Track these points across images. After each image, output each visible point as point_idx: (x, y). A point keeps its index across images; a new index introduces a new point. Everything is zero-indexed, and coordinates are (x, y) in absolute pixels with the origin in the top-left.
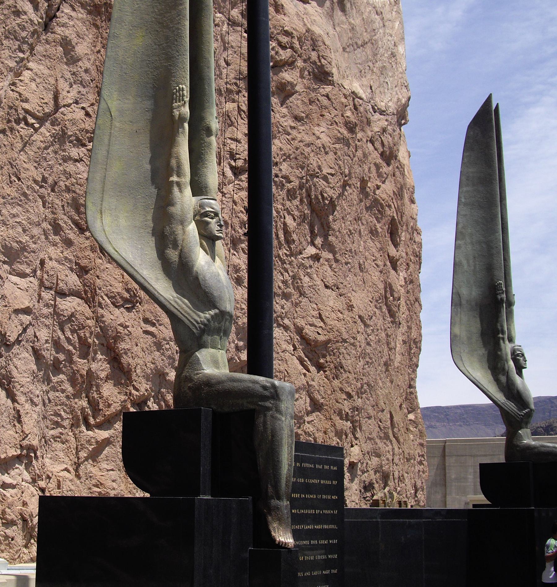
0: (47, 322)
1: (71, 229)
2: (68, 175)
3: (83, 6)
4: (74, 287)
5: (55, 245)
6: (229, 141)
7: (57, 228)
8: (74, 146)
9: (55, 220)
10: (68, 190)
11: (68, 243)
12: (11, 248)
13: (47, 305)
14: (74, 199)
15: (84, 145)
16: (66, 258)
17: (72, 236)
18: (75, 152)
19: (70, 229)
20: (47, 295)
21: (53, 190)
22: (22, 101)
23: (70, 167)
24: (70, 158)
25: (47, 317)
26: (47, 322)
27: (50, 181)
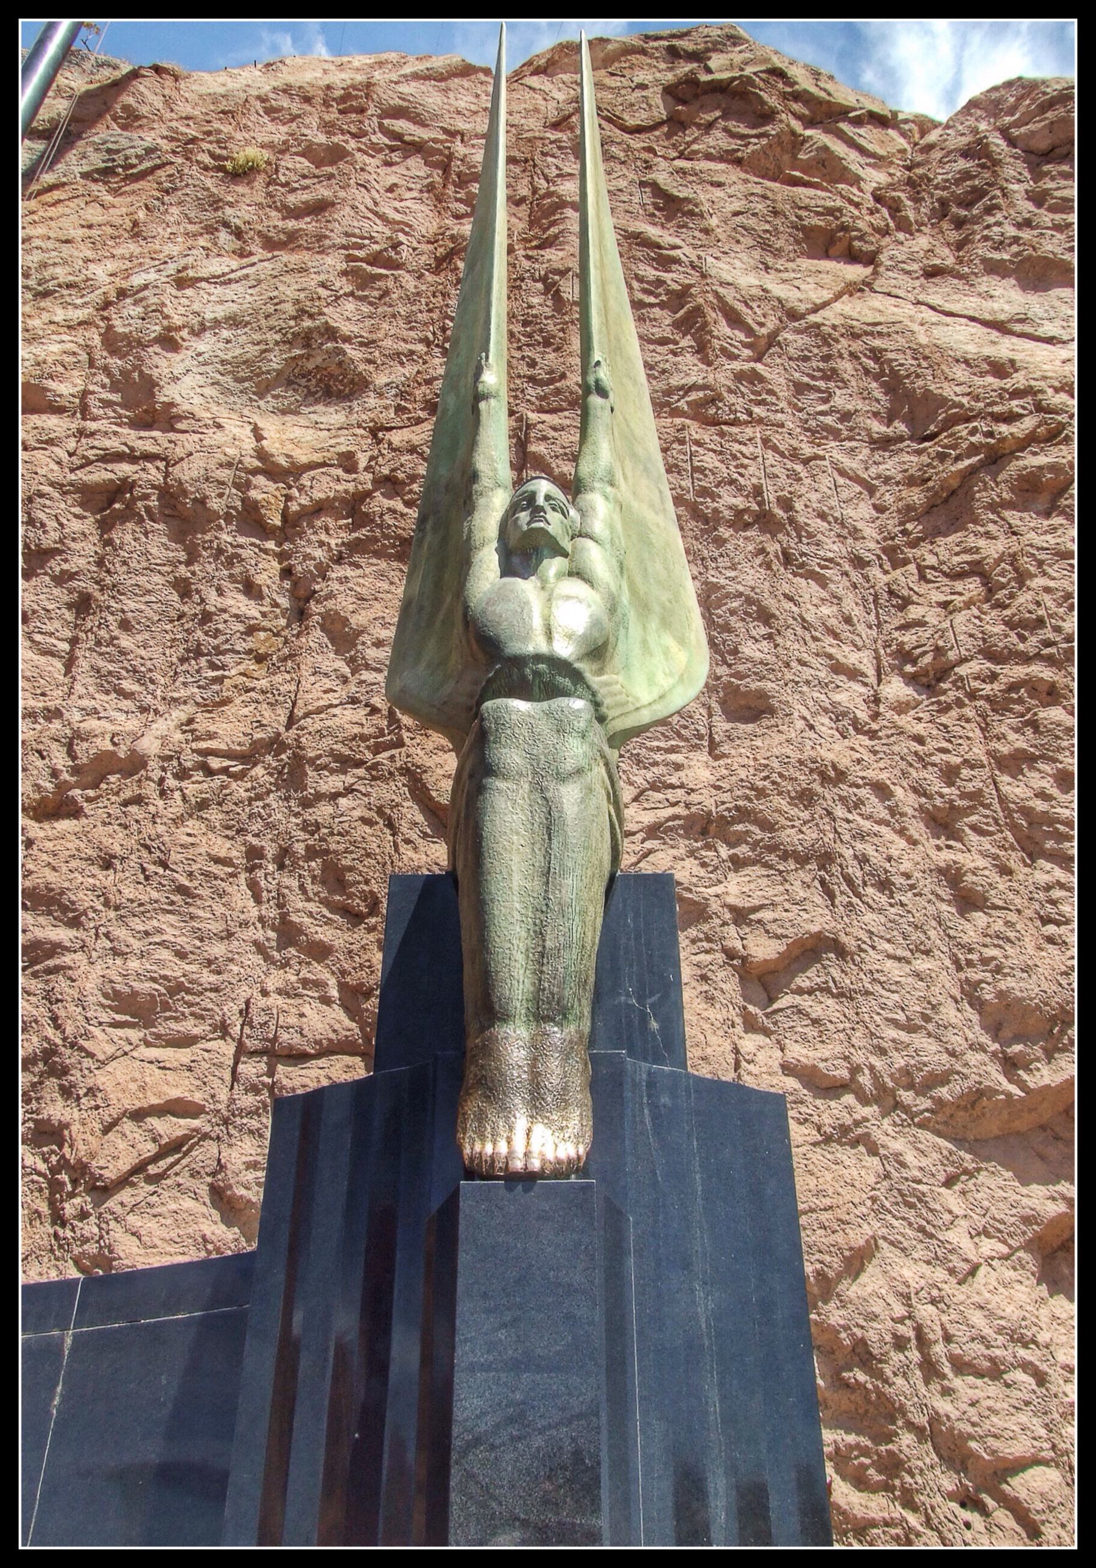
0: (254, 1124)
1: (329, 922)
2: (310, 827)
3: (378, 554)
4: (333, 1036)
5: (285, 965)
6: (896, 634)
7: (288, 933)
8: (332, 772)
9: (284, 917)
10: (312, 853)
11: (320, 952)
12: (135, 994)
13: (254, 1089)
14: (326, 867)
15: (359, 764)
16: (305, 982)
17: (324, 935)
18: (333, 783)
19: (326, 924)
20: (251, 1069)
21: (281, 867)
22: (197, 739)
23: (323, 812)
24: (319, 797)
25: (254, 1113)
26: (254, 1124)
27: (271, 850)
